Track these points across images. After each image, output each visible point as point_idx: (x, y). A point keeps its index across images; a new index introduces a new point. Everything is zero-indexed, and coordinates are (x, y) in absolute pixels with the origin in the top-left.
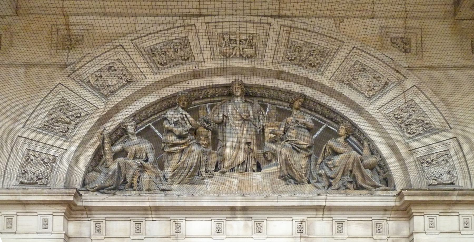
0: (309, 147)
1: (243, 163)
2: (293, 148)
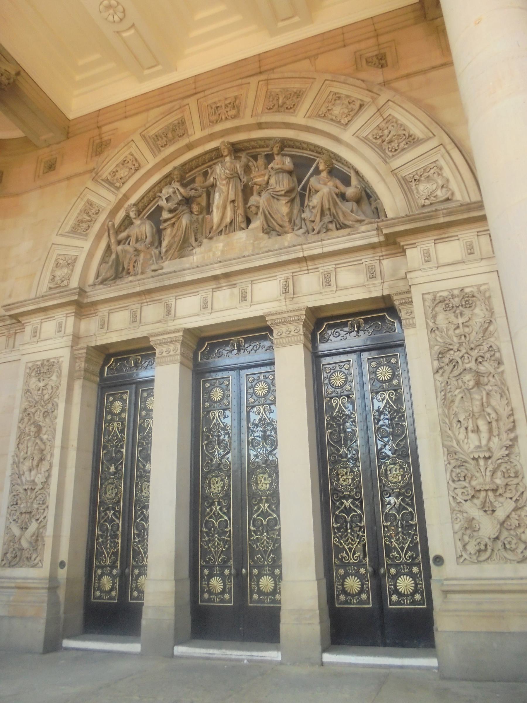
0: (289, 192)
1: (231, 222)
2: (272, 196)
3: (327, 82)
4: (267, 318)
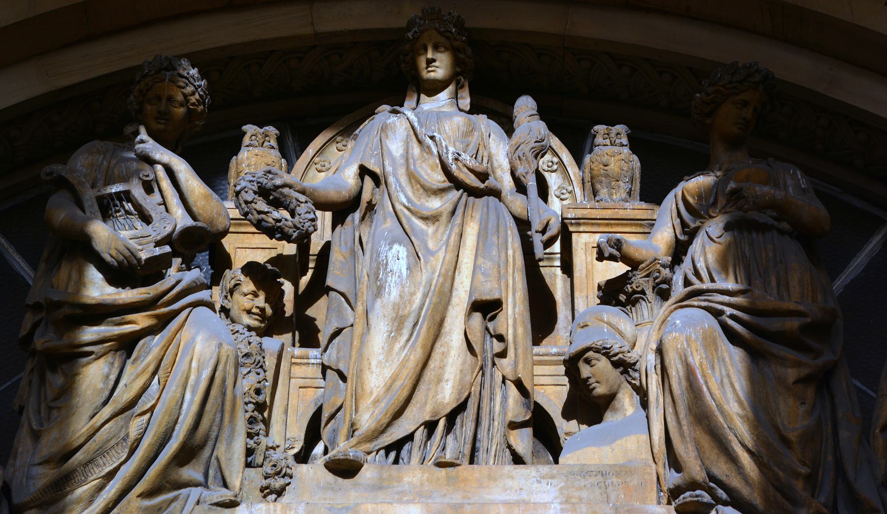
0: (819, 329)
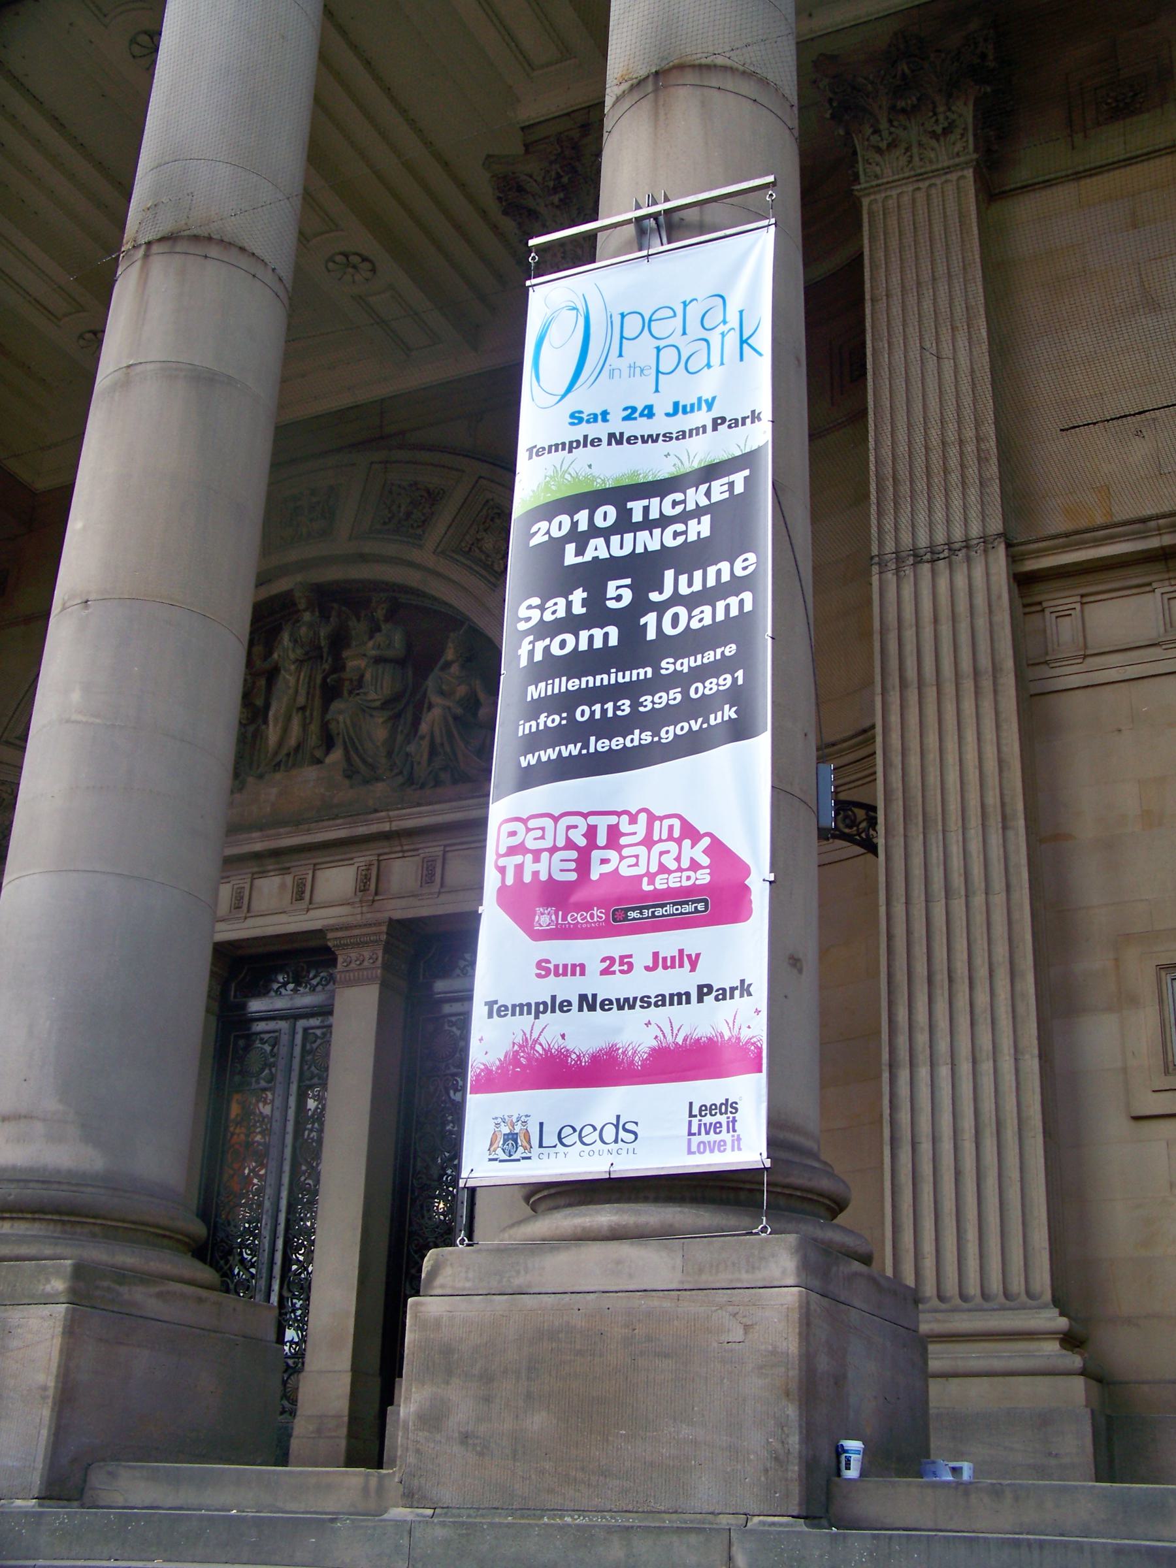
3: (482, 482)
4: (330, 935)
